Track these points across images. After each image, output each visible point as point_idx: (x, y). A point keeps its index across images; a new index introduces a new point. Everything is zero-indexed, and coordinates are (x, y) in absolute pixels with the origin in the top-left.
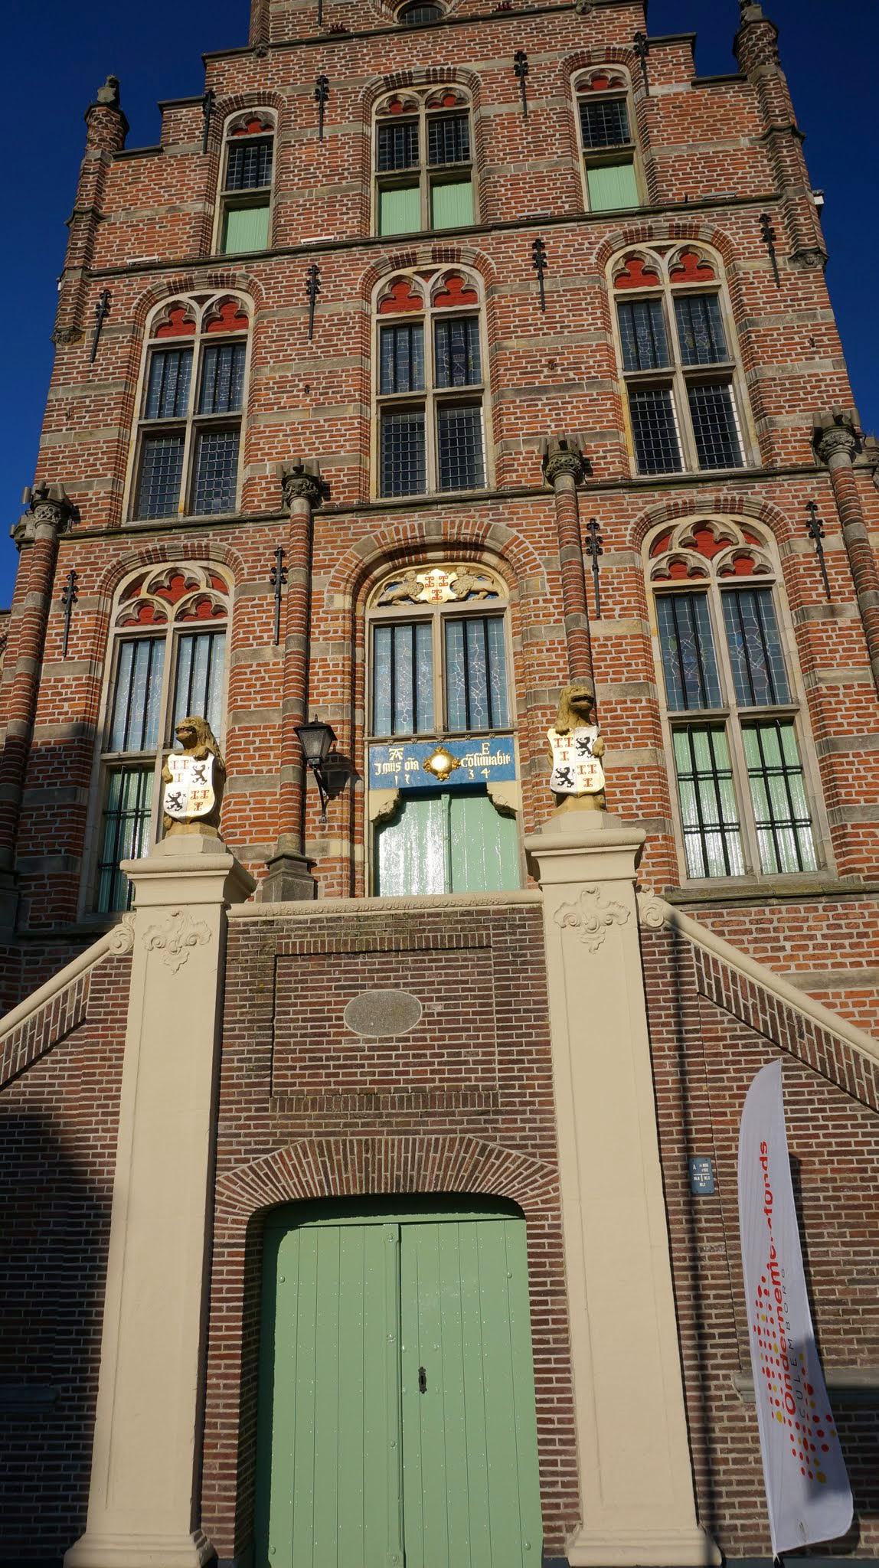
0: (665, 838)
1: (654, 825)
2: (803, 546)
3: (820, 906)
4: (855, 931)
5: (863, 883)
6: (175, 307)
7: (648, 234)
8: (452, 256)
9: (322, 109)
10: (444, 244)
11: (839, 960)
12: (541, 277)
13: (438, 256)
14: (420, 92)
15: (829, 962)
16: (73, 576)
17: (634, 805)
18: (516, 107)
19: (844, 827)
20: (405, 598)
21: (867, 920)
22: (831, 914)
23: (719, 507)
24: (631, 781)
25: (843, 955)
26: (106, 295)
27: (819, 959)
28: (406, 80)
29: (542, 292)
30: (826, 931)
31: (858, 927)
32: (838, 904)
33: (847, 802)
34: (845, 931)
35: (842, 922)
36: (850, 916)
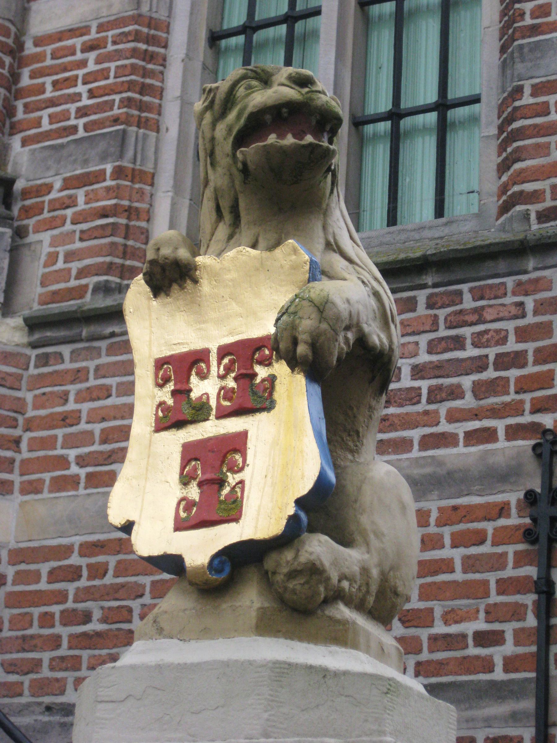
0: (119, 173)
1: (102, 145)
3: (422, 296)
4: (492, 352)
5: (535, 227)
11: (444, 427)
15: (415, 434)
17: (72, 107)
19: (518, 91)
21: (530, 319)
22: (442, 313)
24: (79, 56)
25: (453, 417)
27: (393, 427)
30: (424, 358)
31: (504, 340)
32: (465, 287)
33: (534, 30)
34: (471, 352)
35: (467, 332)
36: (489, 315)
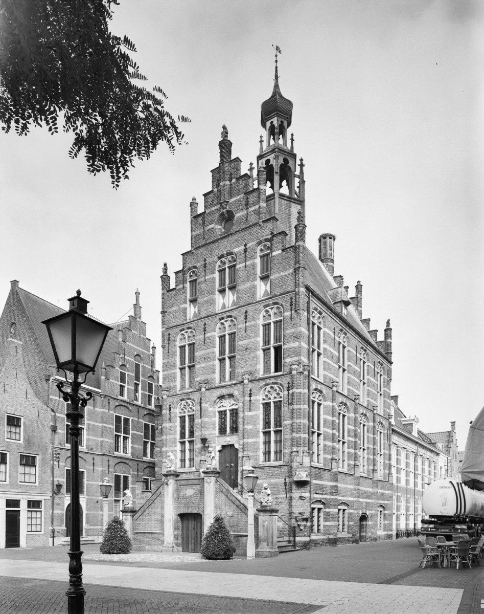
2: (286, 393)
6: (183, 334)
7: (268, 305)
8: (231, 316)
9: (205, 271)
10: (228, 314)
12: (246, 322)
13: (228, 317)
14: (226, 259)
16: (170, 405)
18: (244, 264)
20: (223, 406)
23: (274, 383)
26: (169, 334)
28: (222, 256)
29: (246, 327)
